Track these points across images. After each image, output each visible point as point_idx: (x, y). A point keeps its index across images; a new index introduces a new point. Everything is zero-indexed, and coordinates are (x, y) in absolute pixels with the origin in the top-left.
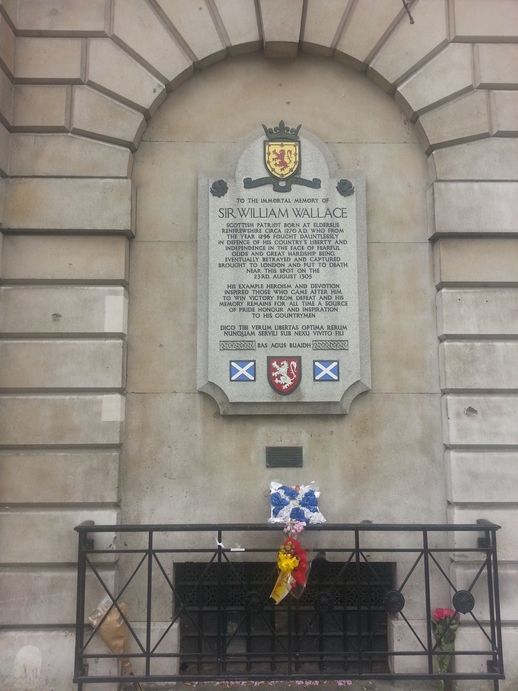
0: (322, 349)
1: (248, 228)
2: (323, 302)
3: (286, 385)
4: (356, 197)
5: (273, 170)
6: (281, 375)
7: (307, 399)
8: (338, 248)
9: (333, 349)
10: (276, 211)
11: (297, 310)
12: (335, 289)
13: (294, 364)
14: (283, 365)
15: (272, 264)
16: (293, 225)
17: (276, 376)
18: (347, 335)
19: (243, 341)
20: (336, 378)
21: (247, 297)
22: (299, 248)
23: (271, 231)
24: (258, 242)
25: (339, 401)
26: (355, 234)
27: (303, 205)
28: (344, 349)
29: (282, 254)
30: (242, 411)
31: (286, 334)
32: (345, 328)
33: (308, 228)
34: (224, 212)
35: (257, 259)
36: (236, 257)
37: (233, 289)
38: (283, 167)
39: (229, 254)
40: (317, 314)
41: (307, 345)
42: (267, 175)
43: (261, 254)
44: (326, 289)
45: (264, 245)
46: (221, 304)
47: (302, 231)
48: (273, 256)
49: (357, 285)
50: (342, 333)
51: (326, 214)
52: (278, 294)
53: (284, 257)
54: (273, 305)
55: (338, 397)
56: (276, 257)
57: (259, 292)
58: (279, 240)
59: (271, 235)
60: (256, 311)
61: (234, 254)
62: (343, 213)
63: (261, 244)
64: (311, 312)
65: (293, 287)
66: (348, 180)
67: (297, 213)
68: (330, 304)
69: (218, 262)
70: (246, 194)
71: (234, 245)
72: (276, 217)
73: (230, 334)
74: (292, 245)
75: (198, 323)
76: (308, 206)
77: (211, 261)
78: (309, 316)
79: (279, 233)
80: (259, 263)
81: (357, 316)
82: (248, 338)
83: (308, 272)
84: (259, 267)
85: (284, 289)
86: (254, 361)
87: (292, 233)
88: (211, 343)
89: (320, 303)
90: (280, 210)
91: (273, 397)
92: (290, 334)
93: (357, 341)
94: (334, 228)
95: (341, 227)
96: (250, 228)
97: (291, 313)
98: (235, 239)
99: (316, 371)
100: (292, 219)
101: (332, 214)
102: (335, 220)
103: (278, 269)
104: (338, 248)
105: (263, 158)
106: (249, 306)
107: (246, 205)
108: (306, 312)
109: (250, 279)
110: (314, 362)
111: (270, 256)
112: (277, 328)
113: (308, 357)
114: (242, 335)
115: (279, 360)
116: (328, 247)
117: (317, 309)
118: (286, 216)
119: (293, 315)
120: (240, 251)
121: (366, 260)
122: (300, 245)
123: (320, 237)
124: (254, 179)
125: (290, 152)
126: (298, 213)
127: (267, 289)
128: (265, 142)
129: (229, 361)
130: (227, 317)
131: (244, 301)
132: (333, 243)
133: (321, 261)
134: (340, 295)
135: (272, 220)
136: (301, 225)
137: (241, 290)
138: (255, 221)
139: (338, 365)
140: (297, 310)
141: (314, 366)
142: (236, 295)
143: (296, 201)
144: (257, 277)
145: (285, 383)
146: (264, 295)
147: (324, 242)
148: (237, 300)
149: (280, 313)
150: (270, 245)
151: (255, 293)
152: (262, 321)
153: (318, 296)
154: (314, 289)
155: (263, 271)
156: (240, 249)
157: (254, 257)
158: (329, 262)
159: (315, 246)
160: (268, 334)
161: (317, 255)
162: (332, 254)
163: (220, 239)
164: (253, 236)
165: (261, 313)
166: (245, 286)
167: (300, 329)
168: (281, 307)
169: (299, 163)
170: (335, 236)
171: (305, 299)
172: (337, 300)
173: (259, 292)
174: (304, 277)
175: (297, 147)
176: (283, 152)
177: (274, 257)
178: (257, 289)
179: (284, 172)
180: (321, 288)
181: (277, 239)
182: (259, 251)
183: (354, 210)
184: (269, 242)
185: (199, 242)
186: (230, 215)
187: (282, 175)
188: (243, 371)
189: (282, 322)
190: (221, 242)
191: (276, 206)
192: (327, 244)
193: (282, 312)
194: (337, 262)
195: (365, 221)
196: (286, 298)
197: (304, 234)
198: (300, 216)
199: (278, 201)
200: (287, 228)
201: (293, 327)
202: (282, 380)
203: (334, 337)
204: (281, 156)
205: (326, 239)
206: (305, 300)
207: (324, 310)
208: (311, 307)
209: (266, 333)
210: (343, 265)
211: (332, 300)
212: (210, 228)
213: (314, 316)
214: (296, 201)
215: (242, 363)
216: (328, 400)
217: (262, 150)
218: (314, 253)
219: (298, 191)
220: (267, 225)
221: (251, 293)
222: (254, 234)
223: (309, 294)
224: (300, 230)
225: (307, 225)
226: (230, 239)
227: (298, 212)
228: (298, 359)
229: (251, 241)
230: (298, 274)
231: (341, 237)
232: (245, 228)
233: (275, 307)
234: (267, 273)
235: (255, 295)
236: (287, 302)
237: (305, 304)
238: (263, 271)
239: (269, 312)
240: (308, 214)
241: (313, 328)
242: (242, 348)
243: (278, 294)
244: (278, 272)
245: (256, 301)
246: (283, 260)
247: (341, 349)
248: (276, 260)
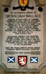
5: (21, 4)
8: (38, 26)
10: (21, 16)
13: (25, 58)
15: (20, 31)
28: (39, 54)
40: (32, 44)
46: (6, 41)
54: (20, 42)
59: (20, 22)
60: (15, 43)
63: (17, 25)
70: (13, 11)
76: (30, 14)
80: (16, 30)
82: (13, 51)
86: (14, 57)
95: (39, 20)
100: (26, 18)
104: (38, 26)
107: (13, 14)
108: (29, 44)
109: (14, 35)
113: (29, 56)
115: (21, 57)
117: (32, 43)
124: (16, 7)
135: (21, 18)
136: (28, 20)
138: (16, 18)
139: (37, 58)
152: (17, 46)
153: (32, 39)
155: (17, 32)
159: (32, 25)
161: (32, 28)
165: (17, 44)
167: (27, 48)
174: (28, 34)
179: (24, 5)
187: (23, 6)
191: (21, 14)
199: (22, 13)
202: (22, 63)
203: (36, 51)
215: (11, 58)
219: (28, 10)
228: (26, 57)
229: (14, 24)
231: (39, 23)
236: (24, 41)
238: (17, 32)
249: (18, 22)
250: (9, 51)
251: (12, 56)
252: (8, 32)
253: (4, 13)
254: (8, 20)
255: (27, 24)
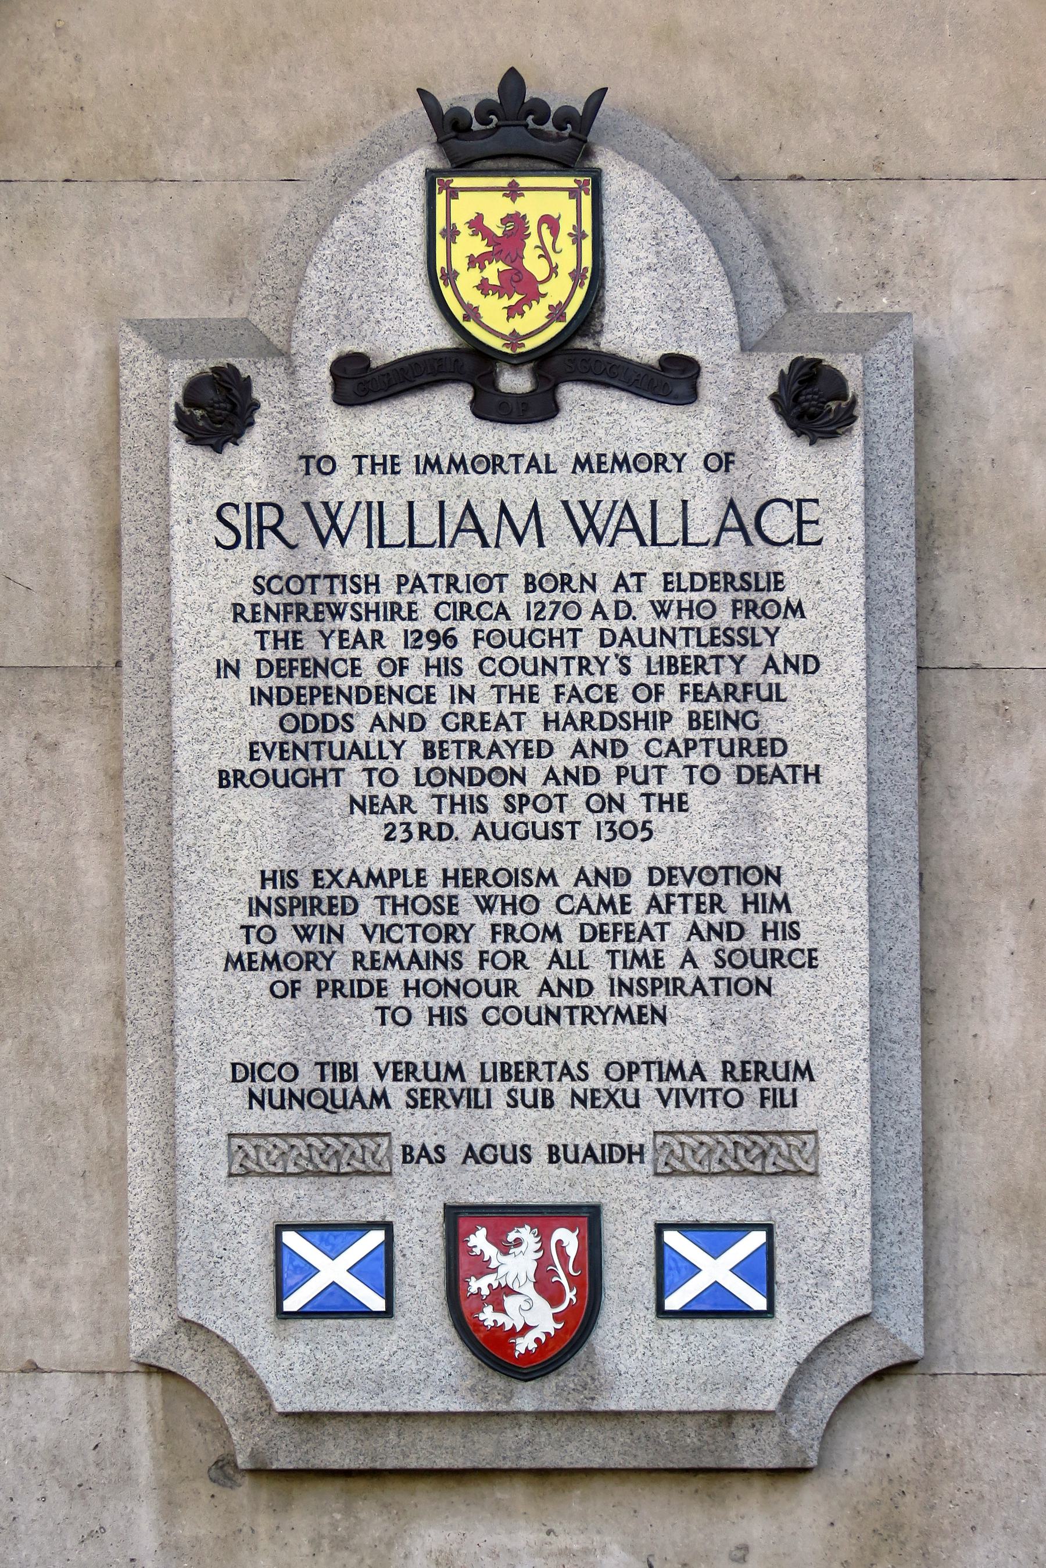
0: (694, 1173)
1: (352, 598)
2: (704, 950)
3: (531, 1336)
4: (868, 448)
5: (472, 313)
6: (509, 1291)
7: (627, 1399)
8: (775, 695)
9: (744, 1172)
11: (584, 987)
12: (762, 889)
13: (569, 1239)
14: (518, 1242)
16: (565, 581)
17: (485, 1292)
18: (810, 1106)
19: (337, 1136)
20: (757, 1302)
21: (352, 926)
22: (595, 694)
23: (464, 611)
24: (401, 666)
25: (771, 1407)
26: (861, 626)
27: (617, 486)
28: (798, 1172)
29: (512, 722)
30: (336, 1454)
31: (529, 1098)
32: (806, 1071)
33: (635, 599)
34: (239, 521)
35: (398, 749)
36: (299, 738)
37: (287, 893)
38: (517, 298)
39: (264, 723)
40: (677, 1006)
41: (630, 1153)
42: (443, 340)
43: (416, 723)
44: (719, 888)
45: (430, 681)
46: (234, 962)
47: (609, 609)
48: (469, 735)
49: (863, 870)
50: (788, 1099)
51: (723, 529)
52: (497, 917)
53: (522, 736)
54: (471, 968)
55: (769, 1391)
56: (485, 740)
57: (408, 904)
58: (499, 654)
59: (464, 629)
60: (395, 998)
61: (290, 724)
62: (800, 523)
63: (414, 676)
64: (648, 1000)
65: (565, 884)
66: (828, 359)
67: (583, 524)
68: (737, 959)
69: (216, 763)
71: (287, 682)
72: (485, 544)
73: (277, 1101)
74: (561, 678)
75: (131, 1052)
76: (637, 488)
77: (182, 759)
78: (639, 1018)
79: (502, 624)
81: (863, 1017)
82: (357, 1120)
83: (635, 809)
84: (406, 785)
85: (521, 891)
86: (387, 1227)
87: (560, 622)
88: (187, 1141)
89: (689, 958)
90: (504, 510)
91: (472, 1389)
92: (548, 1101)
93: (860, 1133)
94: (760, 598)
95: (790, 593)
96: (362, 598)
97: (553, 1003)
98: (295, 654)
99: (666, 1271)
100: (562, 553)
101: (751, 529)
102: (763, 559)
103: (495, 796)
104: (775, 695)
105: (421, 256)
106: (360, 974)
107: (344, 488)
108: (624, 1001)
109: (364, 845)
110: (660, 1228)
111: (459, 735)
112: (489, 1074)
113: (633, 1206)
114: (330, 1104)
115: (502, 1218)
116: (730, 691)
117: (676, 986)
118: (531, 536)
119: (565, 1014)
120: (319, 708)
121: (912, 753)
122: (598, 679)
123: (693, 641)
125: (551, 223)
126: (592, 526)
127: (445, 892)
128: (432, 179)
129: (270, 1228)
130: (263, 1026)
131: (336, 945)
132: (752, 670)
133: (697, 758)
134: (780, 916)
135: (468, 558)
136: (605, 585)
137: (323, 894)
138: (387, 564)
139: (769, 1246)
140: (584, 987)
141: (660, 1245)
142: (299, 920)
143: (581, 464)
144: (400, 833)
145: (527, 1328)
146: (431, 918)
147: (710, 666)
148: (306, 946)
149: (502, 1002)
150: (456, 681)
151: (388, 908)
152: (422, 1043)
153: (679, 922)
154: (662, 890)
155: (425, 808)
156: (319, 701)
157: (385, 737)
158: (736, 760)
159: (671, 683)
160: (449, 1101)
161: (678, 729)
162: (750, 720)
163: (225, 654)
164: (377, 637)
165: (419, 1005)
166: (344, 878)
167: (597, 1080)
168: (510, 973)
169: (596, 280)
170: (761, 636)
171: (621, 938)
172: (771, 944)
173: (408, 904)
174: (616, 832)
175: (587, 200)
176: (516, 224)
177: (478, 736)
178: (398, 891)
179: (522, 325)
180: (696, 887)
181: (490, 652)
182: (408, 708)
183: (857, 509)
184: (451, 667)
185: (126, 665)
186: (269, 536)
187: (515, 338)
188: (333, 1271)
189: (512, 1043)
190: (228, 668)
191: (485, 491)
192: (728, 673)
193: (512, 1000)
194: (770, 761)
195: (911, 561)
196: (530, 932)
197: (618, 627)
198: (599, 539)
199: (495, 463)
200: (539, 595)
201: (566, 1070)
203: (750, 1116)
204: (508, 242)
205: (723, 650)
206: (621, 944)
207: (710, 987)
208: (649, 974)
209: (439, 1099)
210: (800, 773)
211: (745, 944)
212: (177, 598)
213: (663, 1019)
214: (581, 464)
215: (334, 1234)
216: (719, 1402)
217: (419, 217)
218: (665, 718)
220: (442, 582)
221: (368, 911)
222: (381, 625)
223: (638, 915)
224: (599, 609)
225: (632, 582)
226: (271, 654)
227: (590, 517)
228: (589, 1219)
229: (369, 659)
230: (590, 820)
231: (792, 637)
232: (339, 598)
233: (481, 976)
234: (445, 817)
235: (388, 920)
236: (538, 953)
237: (619, 959)
238: (425, 808)
239: (452, 1001)
240: (636, 529)
241: (655, 1074)
242: (333, 1168)
243: (497, 917)
244: (497, 813)
245: (391, 948)
246: (519, 752)
247: (785, 1172)
248: (484, 751)
249: (426, 622)
250: (292, 1119)
251: (338, 1215)
252: (264, 800)
253: (185, 459)
254: (261, 584)
255: (584, 666)
